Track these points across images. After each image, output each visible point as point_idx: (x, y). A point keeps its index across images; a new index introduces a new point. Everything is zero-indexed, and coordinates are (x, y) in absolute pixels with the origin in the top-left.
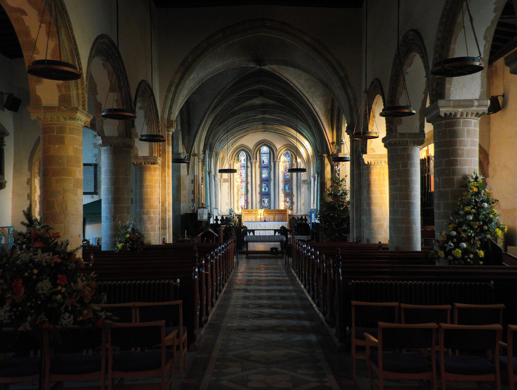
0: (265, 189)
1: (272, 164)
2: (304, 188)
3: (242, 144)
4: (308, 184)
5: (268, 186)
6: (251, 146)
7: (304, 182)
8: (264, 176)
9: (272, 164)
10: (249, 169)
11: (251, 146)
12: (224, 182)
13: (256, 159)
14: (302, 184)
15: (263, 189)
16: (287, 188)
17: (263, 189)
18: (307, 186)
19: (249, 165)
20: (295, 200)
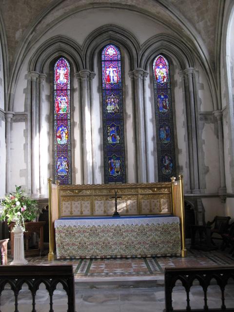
0: (114, 138)
1: (128, 82)
2: (206, 133)
3: (59, 36)
4: (215, 121)
5: (121, 131)
6: (80, 39)
7: (206, 116)
8: (110, 108)
9: (128, 82)
10: (76, 95)
11: (80, 39)
12: (16, 121)
13: (92, 69)
14: (200, 123)
15: (109, 139)
16: (163, 135)
17: (109, 139)
18: (212, 125)
19: (76, 85)
20: (182, 159)
